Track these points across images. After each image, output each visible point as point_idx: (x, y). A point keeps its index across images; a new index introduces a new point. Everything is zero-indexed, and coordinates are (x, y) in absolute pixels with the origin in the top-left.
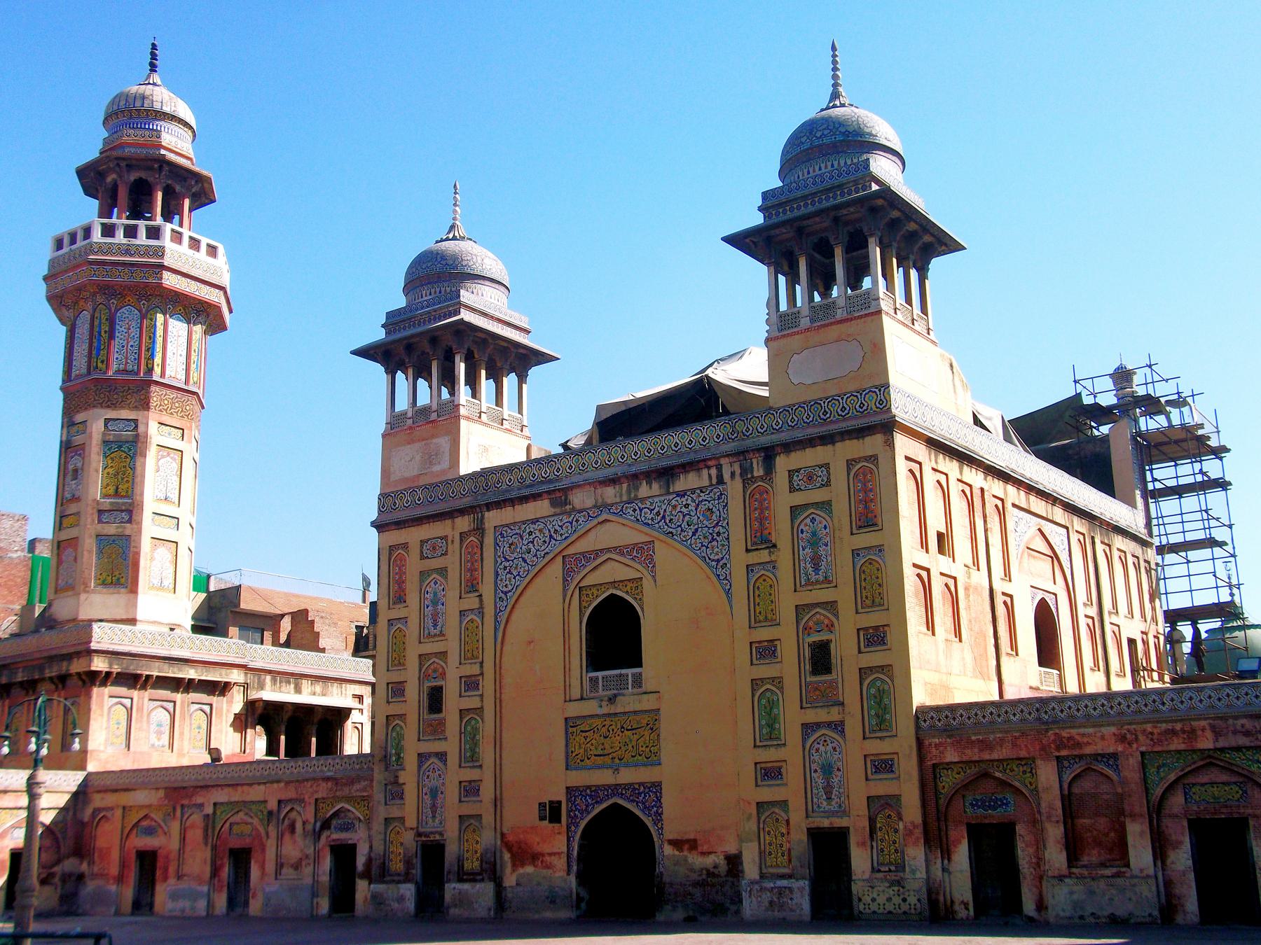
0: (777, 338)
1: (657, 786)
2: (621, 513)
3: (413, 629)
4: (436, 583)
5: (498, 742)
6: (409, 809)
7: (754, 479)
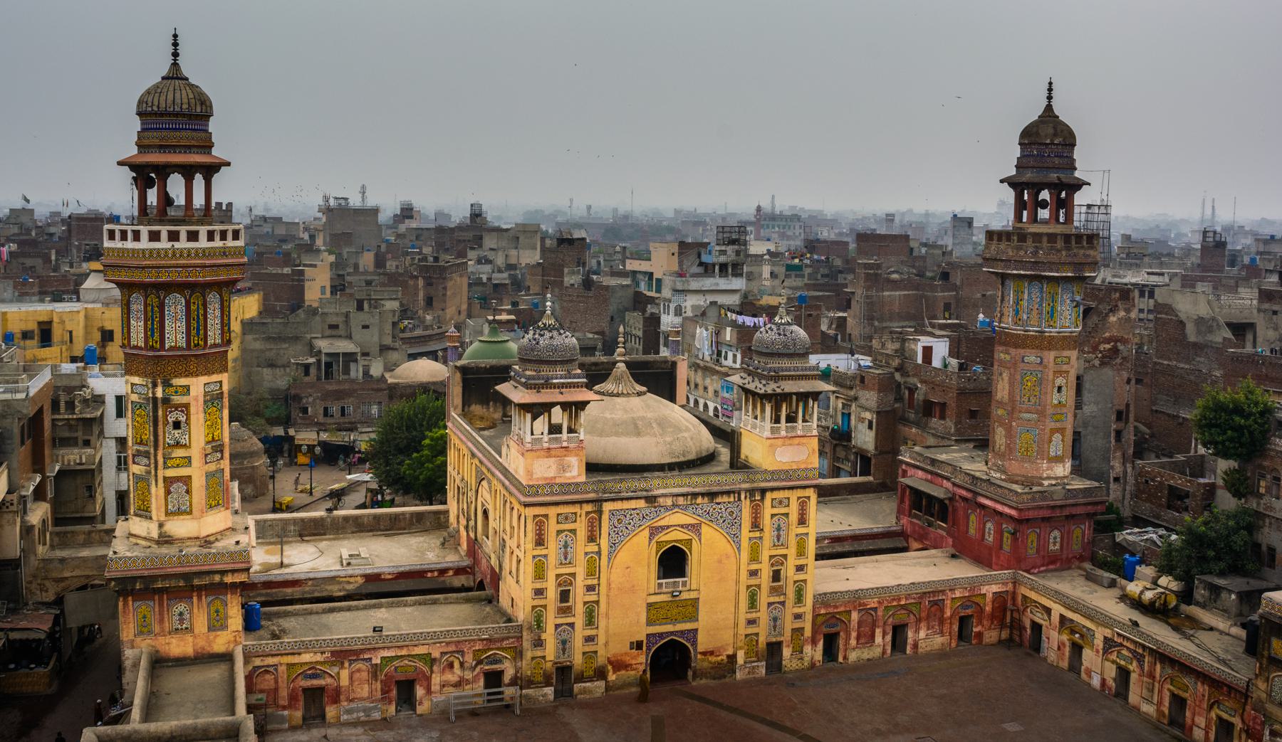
0: (770, 439)
1: (696, 630)
2: (686, 509)
3: (552, 560)
4: (566, 536)
5: (607, 615)
6: (550, 650)
7: (755, 500)
